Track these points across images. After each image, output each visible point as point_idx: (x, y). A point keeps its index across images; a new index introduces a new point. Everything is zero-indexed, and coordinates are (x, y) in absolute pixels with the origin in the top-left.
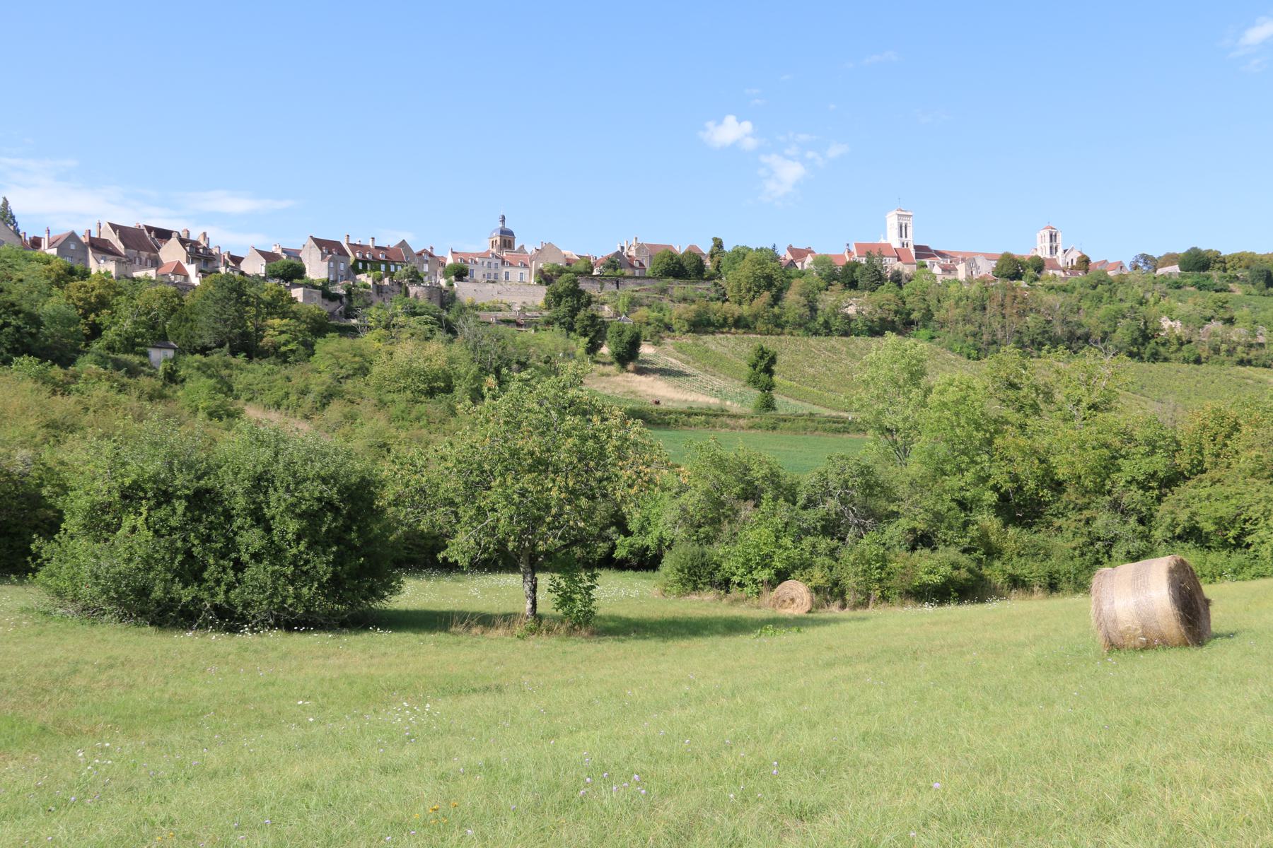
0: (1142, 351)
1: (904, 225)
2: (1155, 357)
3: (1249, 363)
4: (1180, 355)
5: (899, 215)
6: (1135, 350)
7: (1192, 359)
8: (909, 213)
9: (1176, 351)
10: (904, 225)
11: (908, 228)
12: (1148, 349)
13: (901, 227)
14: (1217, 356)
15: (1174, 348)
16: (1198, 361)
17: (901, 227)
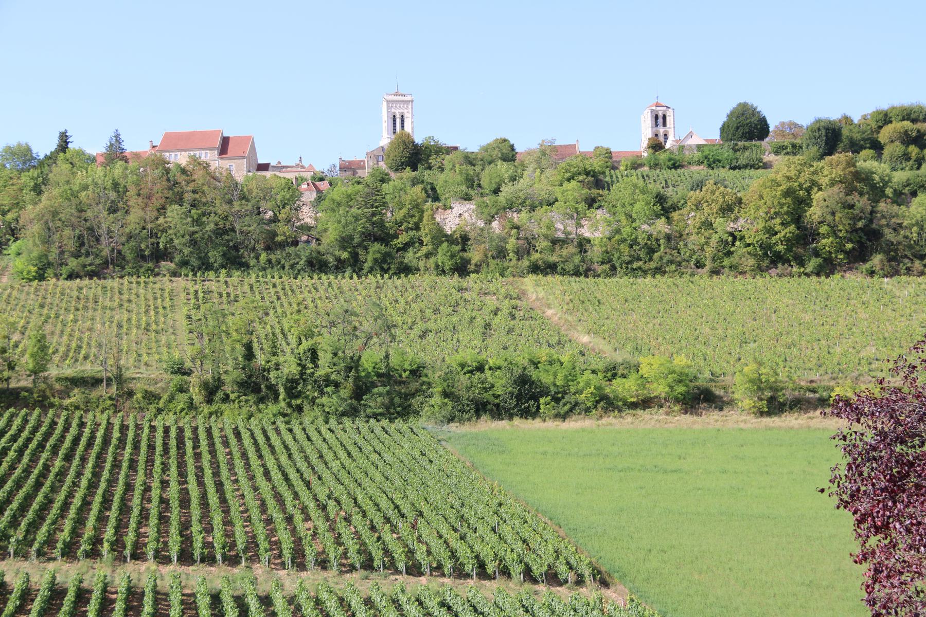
0: (362, 258)
1: (398, 116)
2: (383, 265)
3: (550, 268)
4: (432, 260)
5: (388, 101)
6: (345, 255)
7: (447, 267)
8: (408, 98)
9: (428, 256)
10: (398, 116)
11: (406, 120)
12: (370, 254)
13: (394, 121)
14: (498, 261)
15: (424, 250)
16: (462, 269)
17: (394, 121)
